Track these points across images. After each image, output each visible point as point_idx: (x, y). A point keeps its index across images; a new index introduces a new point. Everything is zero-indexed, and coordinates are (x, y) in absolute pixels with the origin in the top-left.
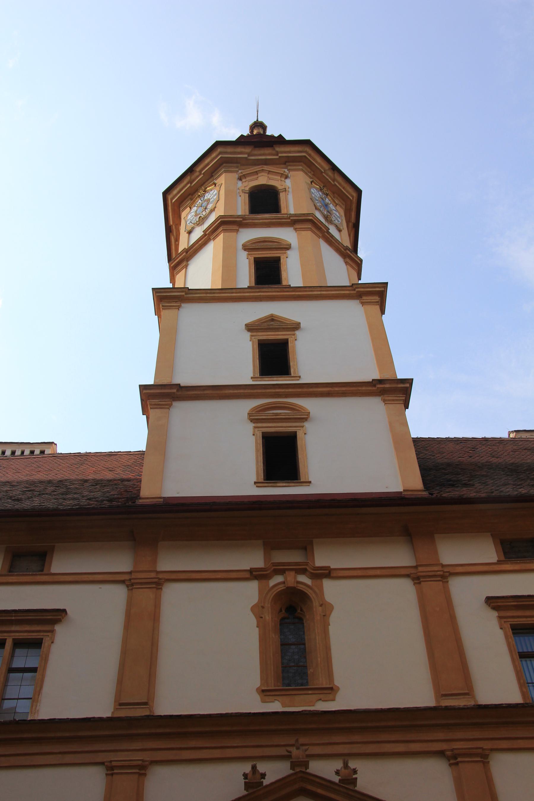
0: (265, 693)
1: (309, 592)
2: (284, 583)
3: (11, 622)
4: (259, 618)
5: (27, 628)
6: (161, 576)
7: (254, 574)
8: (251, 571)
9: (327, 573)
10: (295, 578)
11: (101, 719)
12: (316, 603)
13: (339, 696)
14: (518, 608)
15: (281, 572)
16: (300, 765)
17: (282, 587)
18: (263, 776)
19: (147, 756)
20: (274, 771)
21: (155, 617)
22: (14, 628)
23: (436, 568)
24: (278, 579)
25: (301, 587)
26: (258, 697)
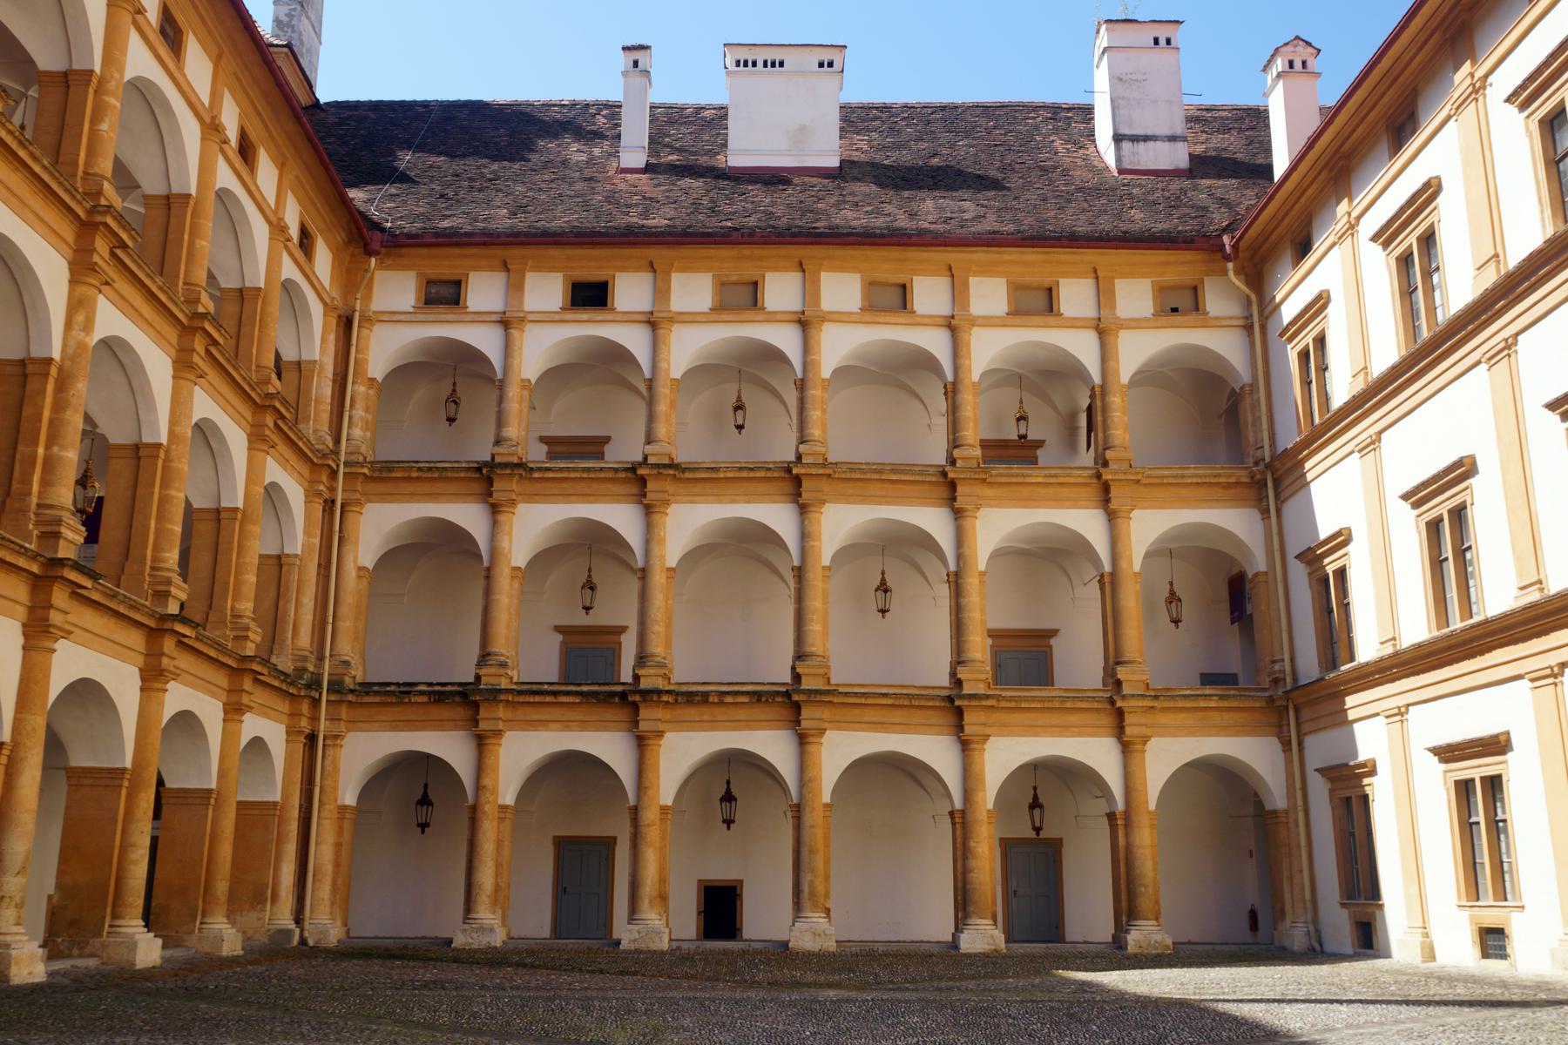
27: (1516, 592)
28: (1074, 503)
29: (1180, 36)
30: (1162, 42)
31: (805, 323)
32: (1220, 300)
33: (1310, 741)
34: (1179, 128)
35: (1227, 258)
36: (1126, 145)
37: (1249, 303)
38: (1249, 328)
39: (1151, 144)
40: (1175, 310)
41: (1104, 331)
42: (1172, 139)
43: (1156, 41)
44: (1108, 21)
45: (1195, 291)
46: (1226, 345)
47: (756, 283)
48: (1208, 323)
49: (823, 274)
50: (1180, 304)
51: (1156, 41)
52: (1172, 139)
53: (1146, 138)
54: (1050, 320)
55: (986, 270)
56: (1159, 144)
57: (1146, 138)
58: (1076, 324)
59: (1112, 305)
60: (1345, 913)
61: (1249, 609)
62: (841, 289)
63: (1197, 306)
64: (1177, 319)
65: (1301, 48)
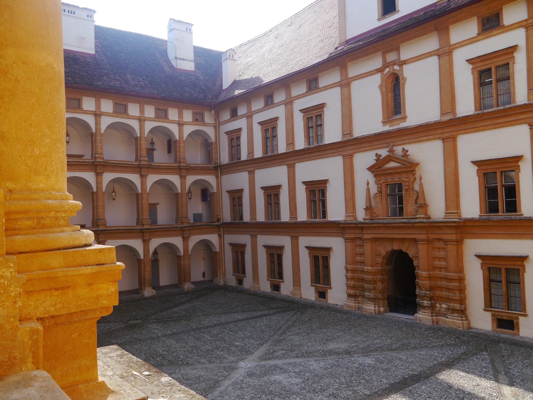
0: (384, 123)
1: (398, 73)
2: (389, 71)
3: (312, 110)
4: (381, 90)
5: (317, 111)
6: (350, 80)
7: (380, 71)
8: (377, 70)
9: (405, 62)
10: (393, 67)
11: (339, 142)
12: (401, 79)
13: (408, 120)
14: (481, 61)
15: (388, 67)
16: (391, 151)
17: (389, 74)
18: (381, 156)
19: (352, 152)
20: (384, 153)
21: (349, 99)
22: (314, 112)
23: (446, 49)
24: (387, 70)
25: (396, 72)
26: (382, 124)
27: (289, 218)
28: (171, 174)
29: (194, 29)
30: (188, 30)
31: (97, 115)
32: (208, 118)
33: (226, 236)
34: (192, 57)
35: (213, 109)
36: (178, 60)
37: (215, 120)
38: (215, 127)
39: (185, 61)
40: (197, 120)
41: (181, 125)
42: (190, 61)
43: (187, 29)
44: (174, 20)
45: (202, 115)
46: (210, 131)
47: (79, 100)
48: (205, 124)
49: (101, 99)
50: (198, 119)
51: (187, 29)
52: (190, 61)
53: (183, 60)
54: (166, 121)
55: (149, 104)
56: (187, 62)
57: (183, 60)
58: (173, 122)
59: (182, 118)
60: (234, 277)
61: (209, 199)
62: (107, 106)
63: (203, 119)
64: (198, 123)
65: (232, 52)
